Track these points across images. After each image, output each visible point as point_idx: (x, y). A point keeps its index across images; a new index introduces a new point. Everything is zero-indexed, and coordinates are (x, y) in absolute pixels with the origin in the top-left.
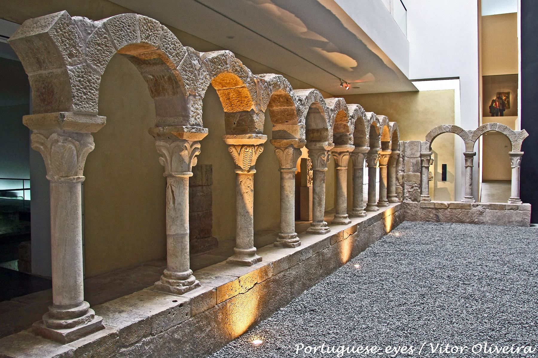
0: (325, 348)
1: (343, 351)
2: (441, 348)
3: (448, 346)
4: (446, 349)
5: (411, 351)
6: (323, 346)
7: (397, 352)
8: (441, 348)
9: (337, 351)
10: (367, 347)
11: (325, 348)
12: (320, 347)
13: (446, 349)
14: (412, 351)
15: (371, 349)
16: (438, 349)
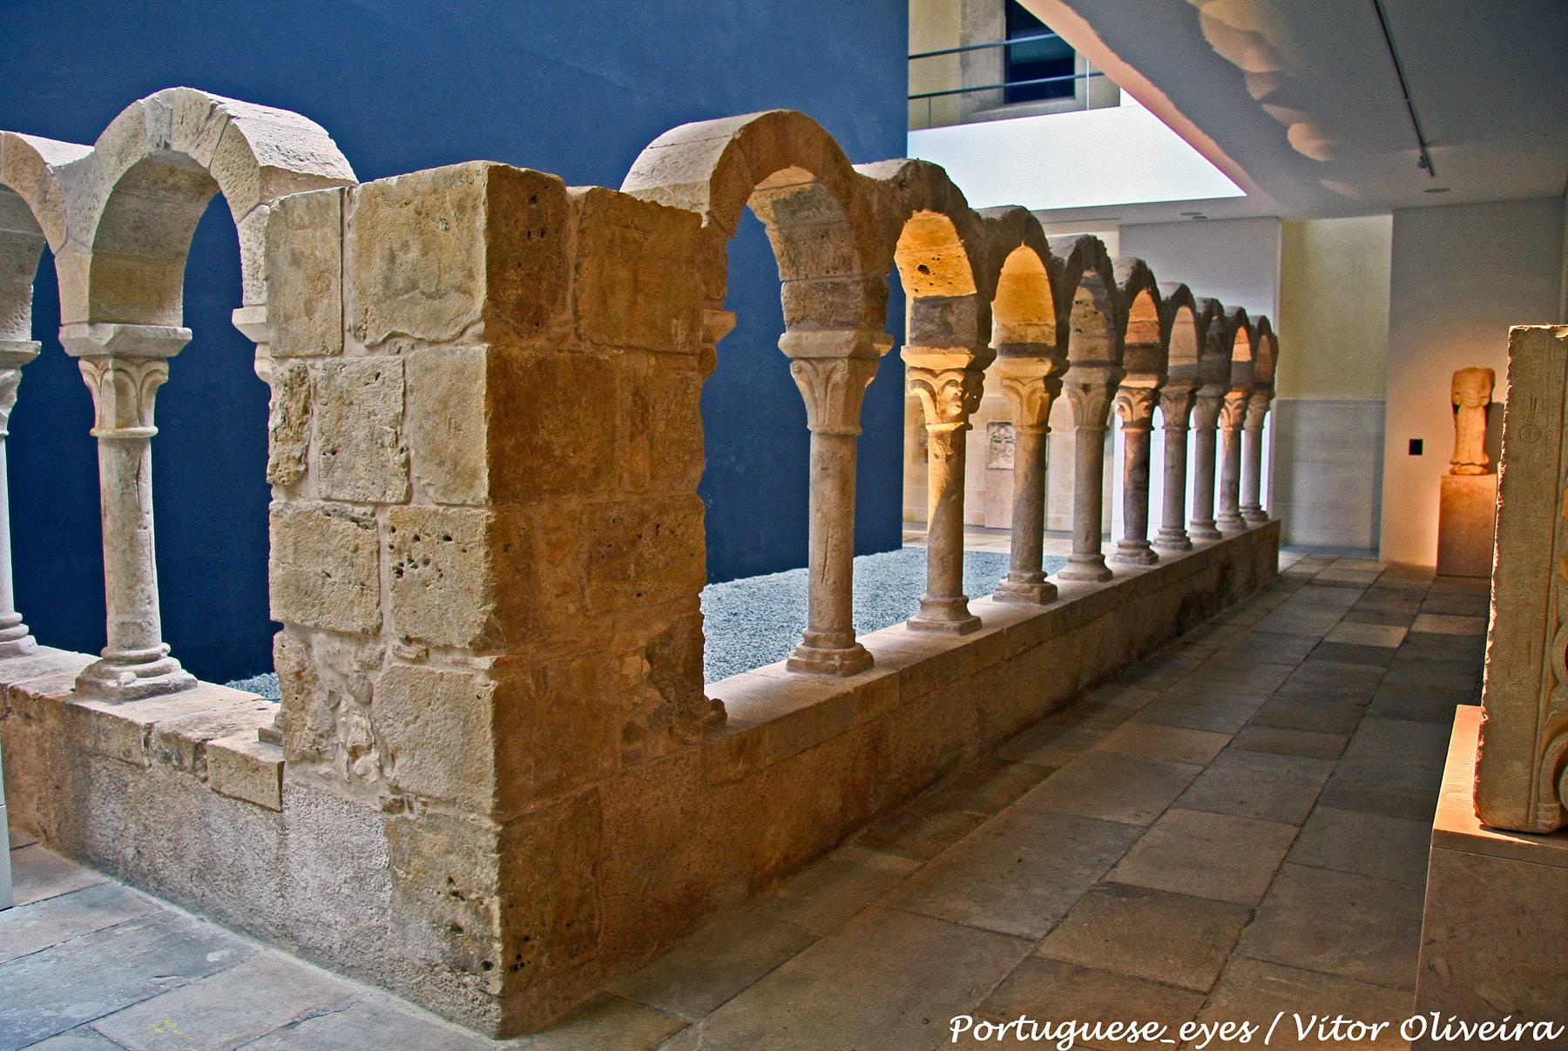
0: (1026, 1029)
1: (1072, 1033)
2: (1322, 1027)
3: (1339, 1021)
4: (1335, 1031)
5: (1247, 1033)
6: (1022, 1021)
7: (1209, 1037)
8: (1322, 1027)
9: (1058, 1034)
10: (1134, 1024)
11: (1026, 1029)
12: (1013, 1024)
13: (1335, 1031)
14: (1249, 1035)
15: (1145, 1030)
16: (1316, 1028)
